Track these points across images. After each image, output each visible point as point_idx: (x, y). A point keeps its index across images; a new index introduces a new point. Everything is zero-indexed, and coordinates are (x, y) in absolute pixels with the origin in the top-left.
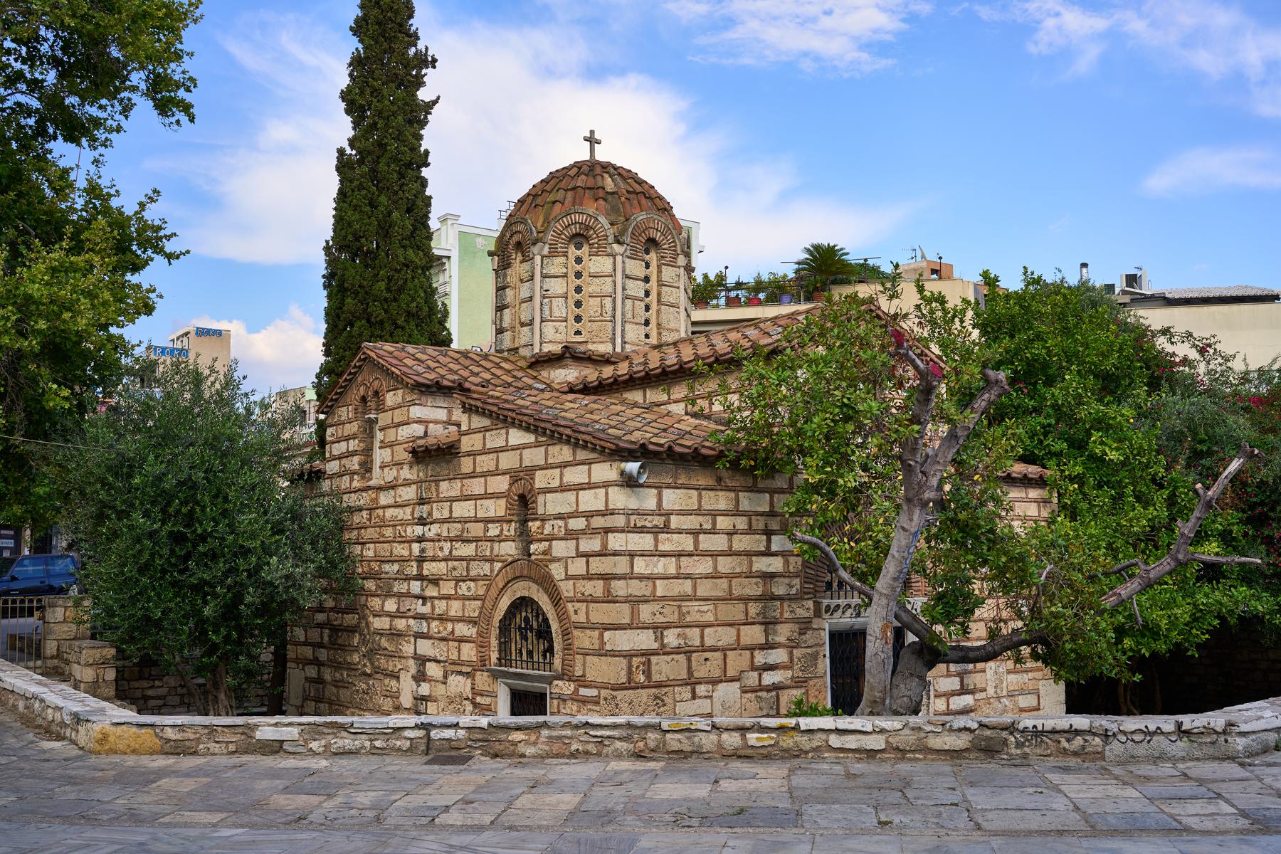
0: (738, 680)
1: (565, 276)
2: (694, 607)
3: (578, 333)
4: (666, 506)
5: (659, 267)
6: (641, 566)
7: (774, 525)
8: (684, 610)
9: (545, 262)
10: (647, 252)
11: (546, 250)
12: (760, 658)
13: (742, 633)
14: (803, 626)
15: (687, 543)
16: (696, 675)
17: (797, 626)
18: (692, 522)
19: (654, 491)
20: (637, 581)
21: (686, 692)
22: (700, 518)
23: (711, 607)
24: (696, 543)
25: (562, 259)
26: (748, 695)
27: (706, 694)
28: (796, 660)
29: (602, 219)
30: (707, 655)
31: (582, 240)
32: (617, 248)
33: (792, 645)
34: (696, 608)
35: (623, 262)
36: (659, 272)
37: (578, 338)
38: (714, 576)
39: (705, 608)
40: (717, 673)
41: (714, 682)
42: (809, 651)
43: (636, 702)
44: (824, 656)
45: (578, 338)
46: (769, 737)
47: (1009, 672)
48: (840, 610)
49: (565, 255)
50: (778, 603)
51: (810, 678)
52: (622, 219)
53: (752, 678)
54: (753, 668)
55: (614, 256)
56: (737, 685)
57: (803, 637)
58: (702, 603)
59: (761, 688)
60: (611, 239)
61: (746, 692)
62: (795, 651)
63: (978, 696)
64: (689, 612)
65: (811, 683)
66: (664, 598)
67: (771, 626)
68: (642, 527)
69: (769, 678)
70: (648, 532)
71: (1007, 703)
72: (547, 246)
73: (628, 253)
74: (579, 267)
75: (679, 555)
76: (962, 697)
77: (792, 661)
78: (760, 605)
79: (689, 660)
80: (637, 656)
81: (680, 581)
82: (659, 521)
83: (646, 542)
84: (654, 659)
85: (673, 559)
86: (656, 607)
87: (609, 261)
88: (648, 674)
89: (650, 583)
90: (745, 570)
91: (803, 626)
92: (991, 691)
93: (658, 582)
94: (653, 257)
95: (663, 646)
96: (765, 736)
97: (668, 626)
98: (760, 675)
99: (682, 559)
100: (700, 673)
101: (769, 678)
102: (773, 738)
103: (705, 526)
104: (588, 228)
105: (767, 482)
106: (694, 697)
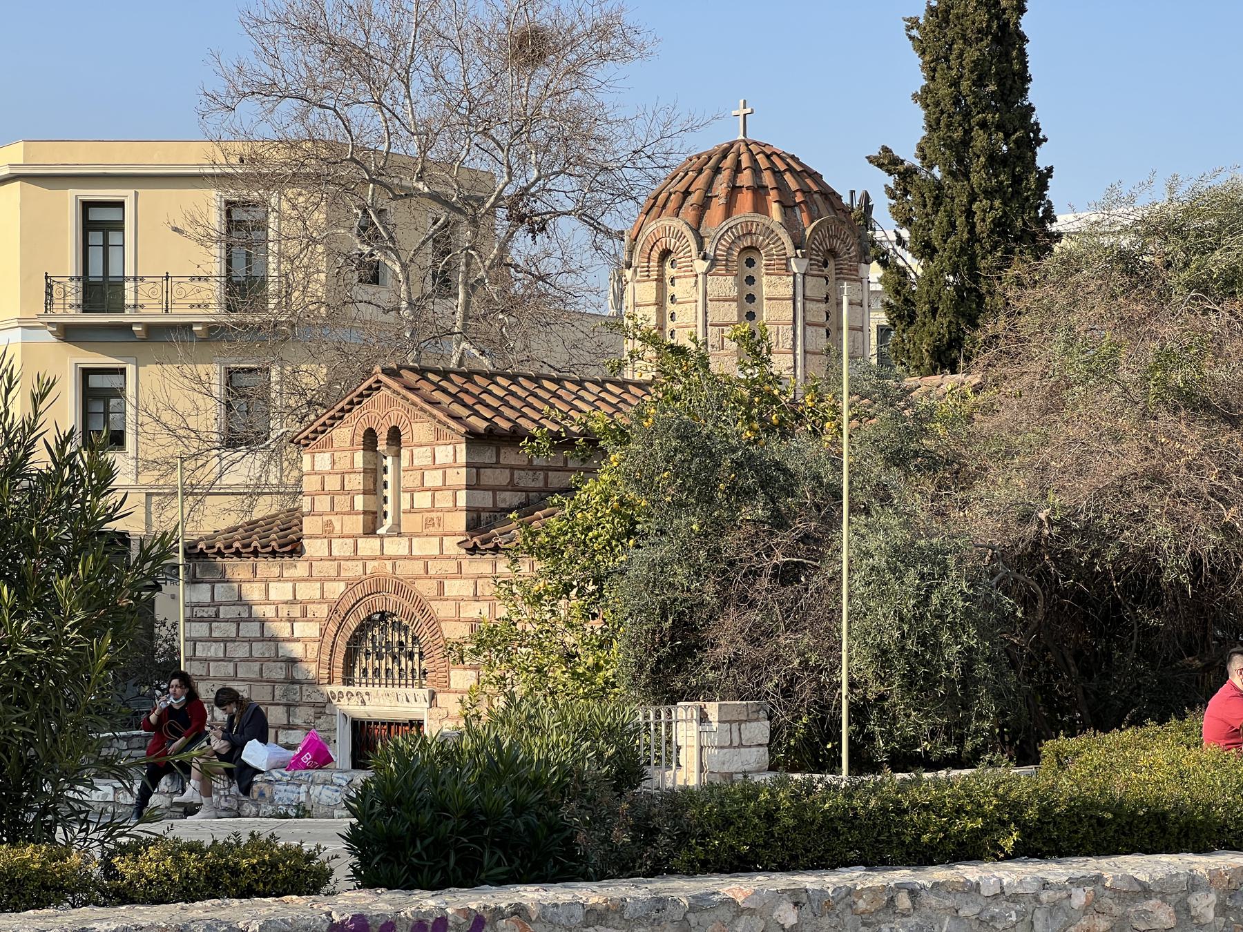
14: (319, 710)
15: (231, 630)
19: (209, 586)
22: (240, 608)
23: (247, 687)
38: (250, 659)
50: (298, 687)
58: (240, 683)
68: (202, 617)
91: (319, 710)
93: (211, 663)
99: (228, 644)
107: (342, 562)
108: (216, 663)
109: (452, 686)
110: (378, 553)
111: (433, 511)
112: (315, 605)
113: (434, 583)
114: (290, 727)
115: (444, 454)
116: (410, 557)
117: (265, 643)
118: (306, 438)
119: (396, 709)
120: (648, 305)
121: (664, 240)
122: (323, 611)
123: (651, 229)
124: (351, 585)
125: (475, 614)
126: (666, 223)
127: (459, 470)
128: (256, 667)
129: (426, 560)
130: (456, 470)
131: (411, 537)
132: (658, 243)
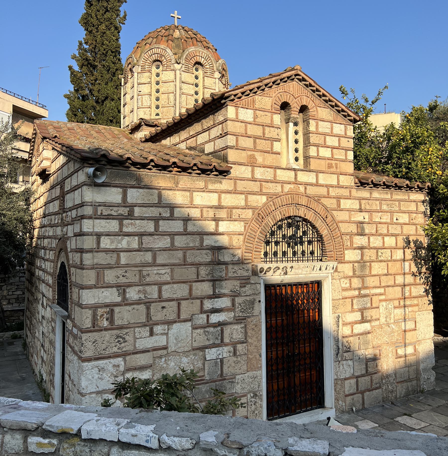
0: (190, 320)
1: (150, 83)
2: (155, 270)
3: (157, 115)
4: (130, 200)
5: (203, 78)
6: (106, 243)
7: (223, 214)
8: (145, 273)
9: (139, 76)
10: (197, 70)
11: (139, 70)
12: (208, 305)
13: (194, 288)
14: (243, 281)
15: (150, 227)
16: (154, 318)
17: (239, 282)
18: (154, 212)
19: (120, 190)
20: (104, 253)
21: (145, 331)
22: (161, 210)
23: (169, 271)
24: (157, 227)
25: (147, 74)
26: (199, 331)
27: (162, 332)
28: (237, 305)
29: (168, 50)
30: (164, 304)
31: (158, 63)
32: (177, 66)
33: (234, 295)
34: (155, 272)
35: (180, 74)
36: (204, 81)
37: (157, 117)
38: (172, 248)
39: (163, 272)
40: (173, 317)
41: (170, 323)
42: (248, 298)
43: (100, 341)
44: (260, 301)
45: (157, 117)
46: (50, 443)
47: (395, 308)
48: (272, 271)
49: (150, 71)
51: (249, 317)
52: (181, 51)
53: (201, 319)
54: (202, 311)
55: (174, 70)
56: (189, 324)
57: (243, 289)
59: (209, 325)
60: (173, 61)
61: (196, 328)
62: (237, 299)
63: (374, 324)
64: (148, 275)
65: (249, 320)
66: (127, 265)
67: (217, 282)
68: (108, 215)
69: (215, 318)
70: (113, 219)
71: (394, 327)
72: (140, 67)
73: (183, 69)
74: (158, 79)
75: (141, 235)
76: (362, 324)
77: (233, 305)
78: (209, 268)
79: (148, 309)
80: (101, 307)
81: (142, 253)
82: (124, 211)
83: (113, 226)
84: (117, 309)
85: (136, 238)
86: (120, 272)
87: (172, 74)
88: (111, 320)
89: (115, 255)
90: (197, 245)
91: (243, 281)
92: (383, 320)
93: (122, 254)
94: (200, 73)
95: (124, 298)
96: (46, 441)
97: (130, 285)
98: (208, 316)
99: (144, 237)
100: (157, 316)
101: (215, 318)
102: (52, 445)
103: (164, 215)
104: (162, 56)
105: (216, 185)
106: (152, 334)
107: (264, 183)
108: (129, 253)
109: (346, 259)
110: (293, 180)
111: (332, 160)
112: (240, 210)
113: (334, 201)
114: (215, 296)
115: (339, 129)
116: (317, 185)
117: (188, 236)
118: (235, 95)
119: (311, 275)
120: (189, 84)
121: (198, 57)
122: (249, 214)
123: (192, 50)
124: (271, 196)
125: (360, 219)
126: (200, 50)
127: (349, 140)
128: (180, 254)
129: (328, 186)
130: (347, 139)
131: (318, 172)
132: (195, 58)
